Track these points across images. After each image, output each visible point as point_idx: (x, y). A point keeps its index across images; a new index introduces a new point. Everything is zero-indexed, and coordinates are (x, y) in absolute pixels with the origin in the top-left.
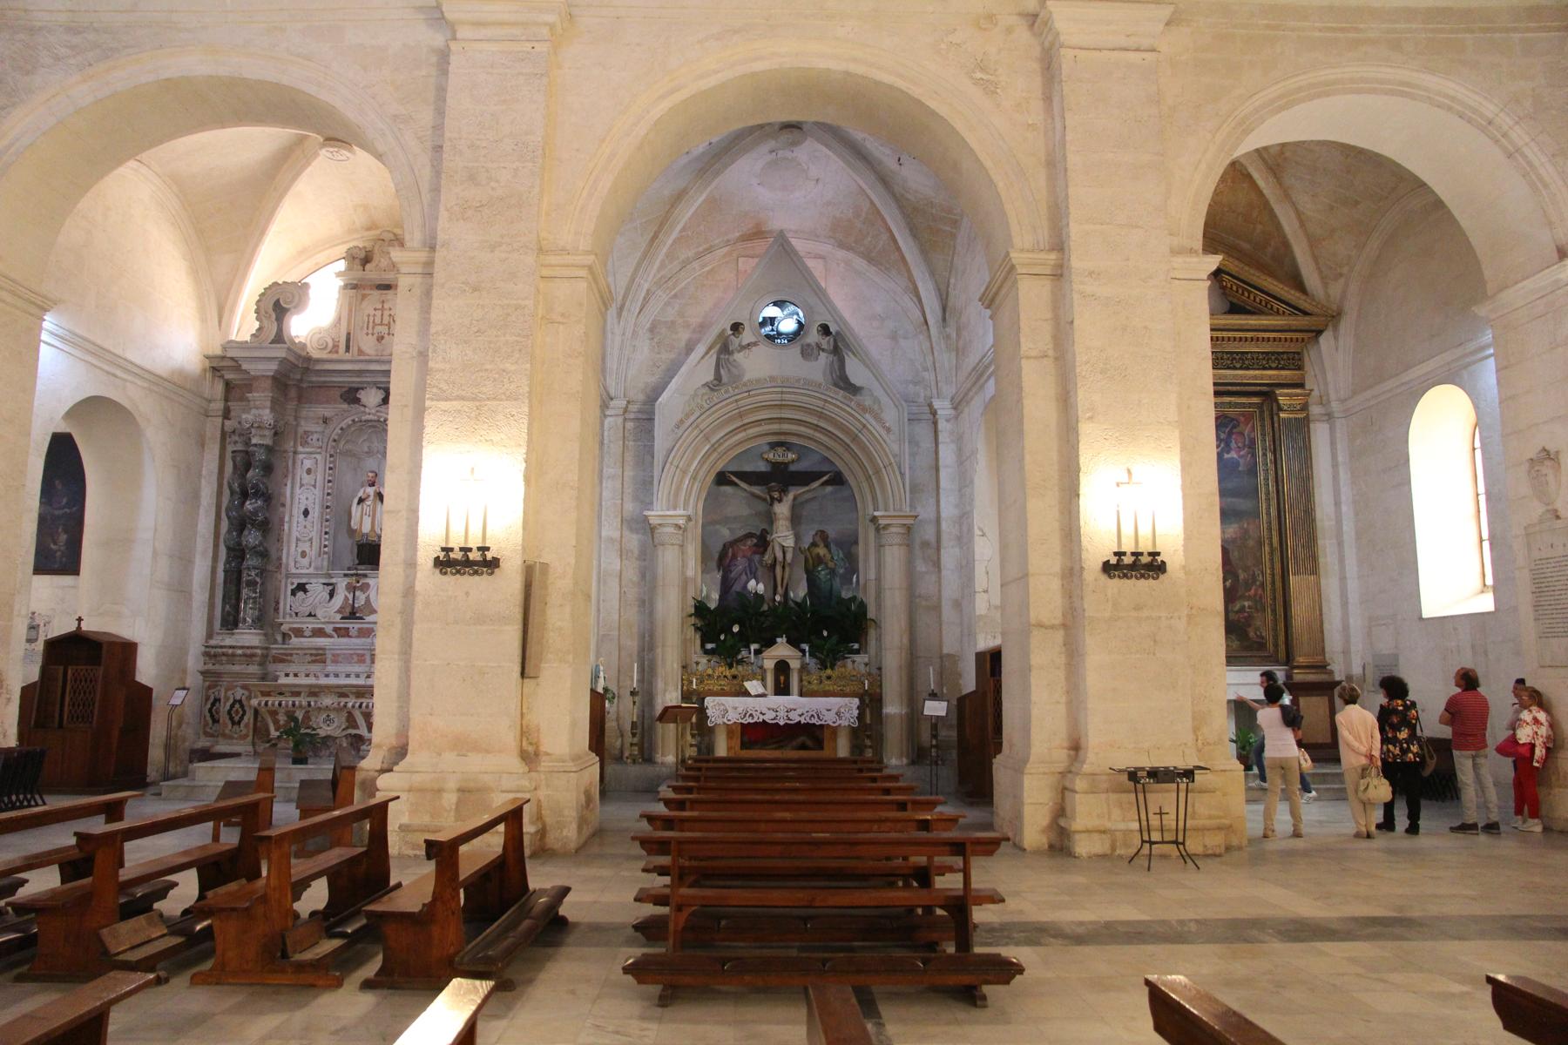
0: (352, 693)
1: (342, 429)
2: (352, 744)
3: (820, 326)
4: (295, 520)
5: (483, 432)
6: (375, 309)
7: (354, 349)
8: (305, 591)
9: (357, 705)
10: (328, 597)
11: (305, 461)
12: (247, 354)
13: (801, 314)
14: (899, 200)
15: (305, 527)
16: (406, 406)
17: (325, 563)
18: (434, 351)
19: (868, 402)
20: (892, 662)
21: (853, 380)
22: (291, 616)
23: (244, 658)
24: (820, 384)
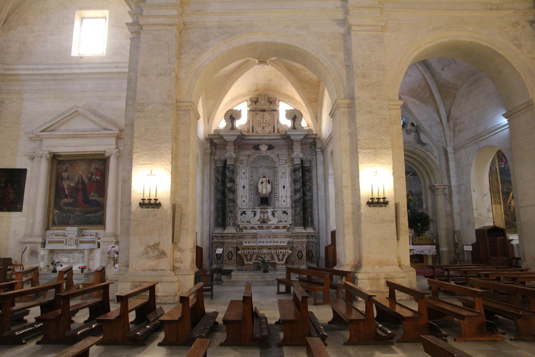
0: (273, 248)
1: (254, 159)
3: (411, 123)
4: (240, 190)
5: (378, 160)
6: (261, 118)
7: (255, 131)
8: (245, 214)
9: (275, 252)
10: (253, 216)
11: (242, 170)
12: (226, 134)
13: (404, 119)
14: (436, 82)
15: (244, 192)
16: (347, 151)
17: (252, 204)
18: (359, 133)
19: (428, 148)
20: (442, 233)
21: (424, 141)
22: (241, 222)
23: (231, 237)
24: (413, 143)
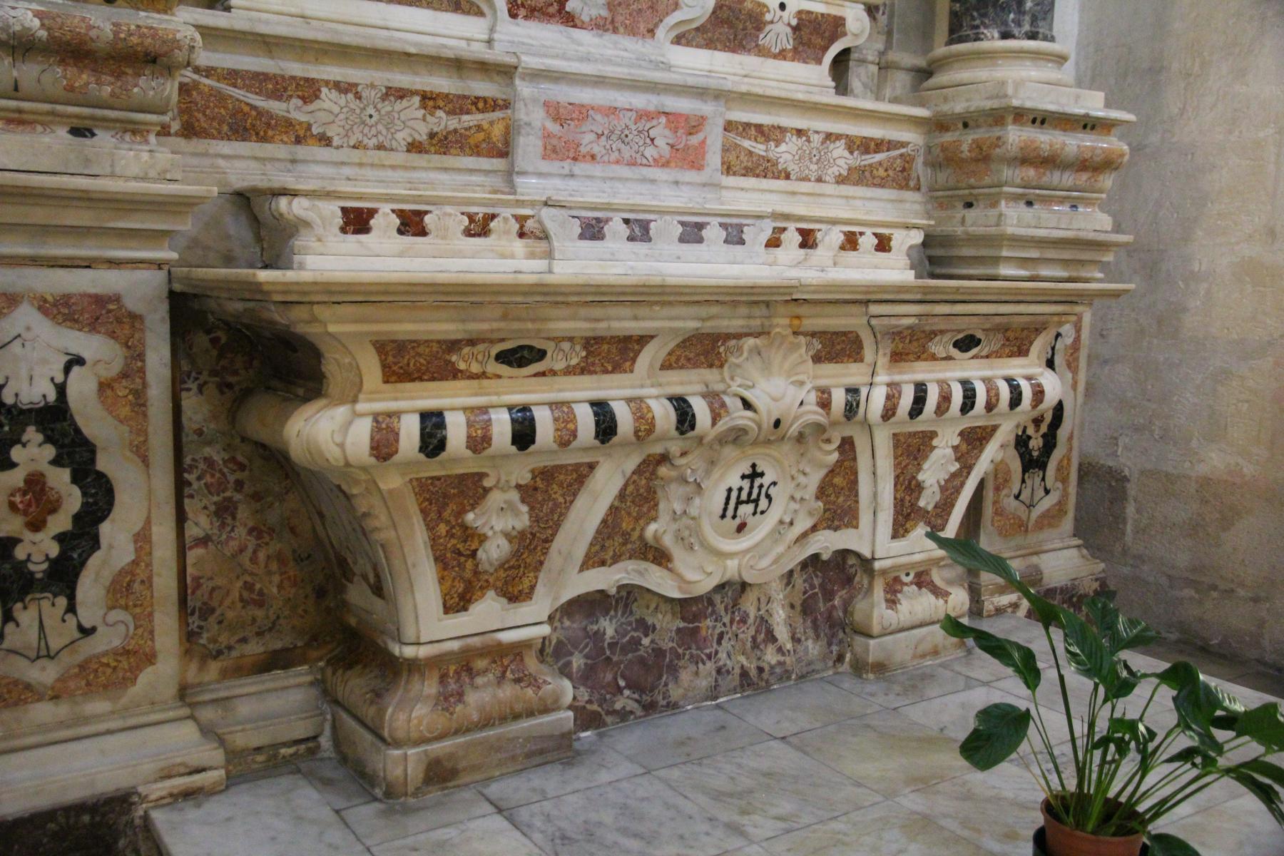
2: (807, 609)
23: (53, 76)
